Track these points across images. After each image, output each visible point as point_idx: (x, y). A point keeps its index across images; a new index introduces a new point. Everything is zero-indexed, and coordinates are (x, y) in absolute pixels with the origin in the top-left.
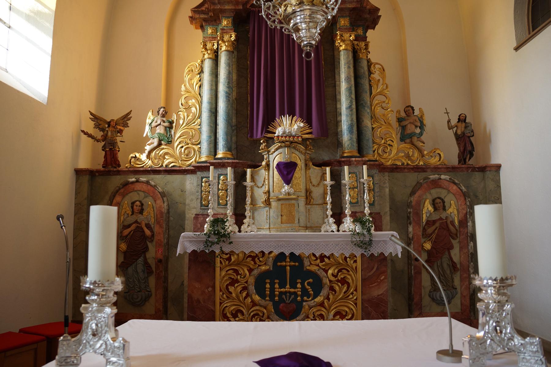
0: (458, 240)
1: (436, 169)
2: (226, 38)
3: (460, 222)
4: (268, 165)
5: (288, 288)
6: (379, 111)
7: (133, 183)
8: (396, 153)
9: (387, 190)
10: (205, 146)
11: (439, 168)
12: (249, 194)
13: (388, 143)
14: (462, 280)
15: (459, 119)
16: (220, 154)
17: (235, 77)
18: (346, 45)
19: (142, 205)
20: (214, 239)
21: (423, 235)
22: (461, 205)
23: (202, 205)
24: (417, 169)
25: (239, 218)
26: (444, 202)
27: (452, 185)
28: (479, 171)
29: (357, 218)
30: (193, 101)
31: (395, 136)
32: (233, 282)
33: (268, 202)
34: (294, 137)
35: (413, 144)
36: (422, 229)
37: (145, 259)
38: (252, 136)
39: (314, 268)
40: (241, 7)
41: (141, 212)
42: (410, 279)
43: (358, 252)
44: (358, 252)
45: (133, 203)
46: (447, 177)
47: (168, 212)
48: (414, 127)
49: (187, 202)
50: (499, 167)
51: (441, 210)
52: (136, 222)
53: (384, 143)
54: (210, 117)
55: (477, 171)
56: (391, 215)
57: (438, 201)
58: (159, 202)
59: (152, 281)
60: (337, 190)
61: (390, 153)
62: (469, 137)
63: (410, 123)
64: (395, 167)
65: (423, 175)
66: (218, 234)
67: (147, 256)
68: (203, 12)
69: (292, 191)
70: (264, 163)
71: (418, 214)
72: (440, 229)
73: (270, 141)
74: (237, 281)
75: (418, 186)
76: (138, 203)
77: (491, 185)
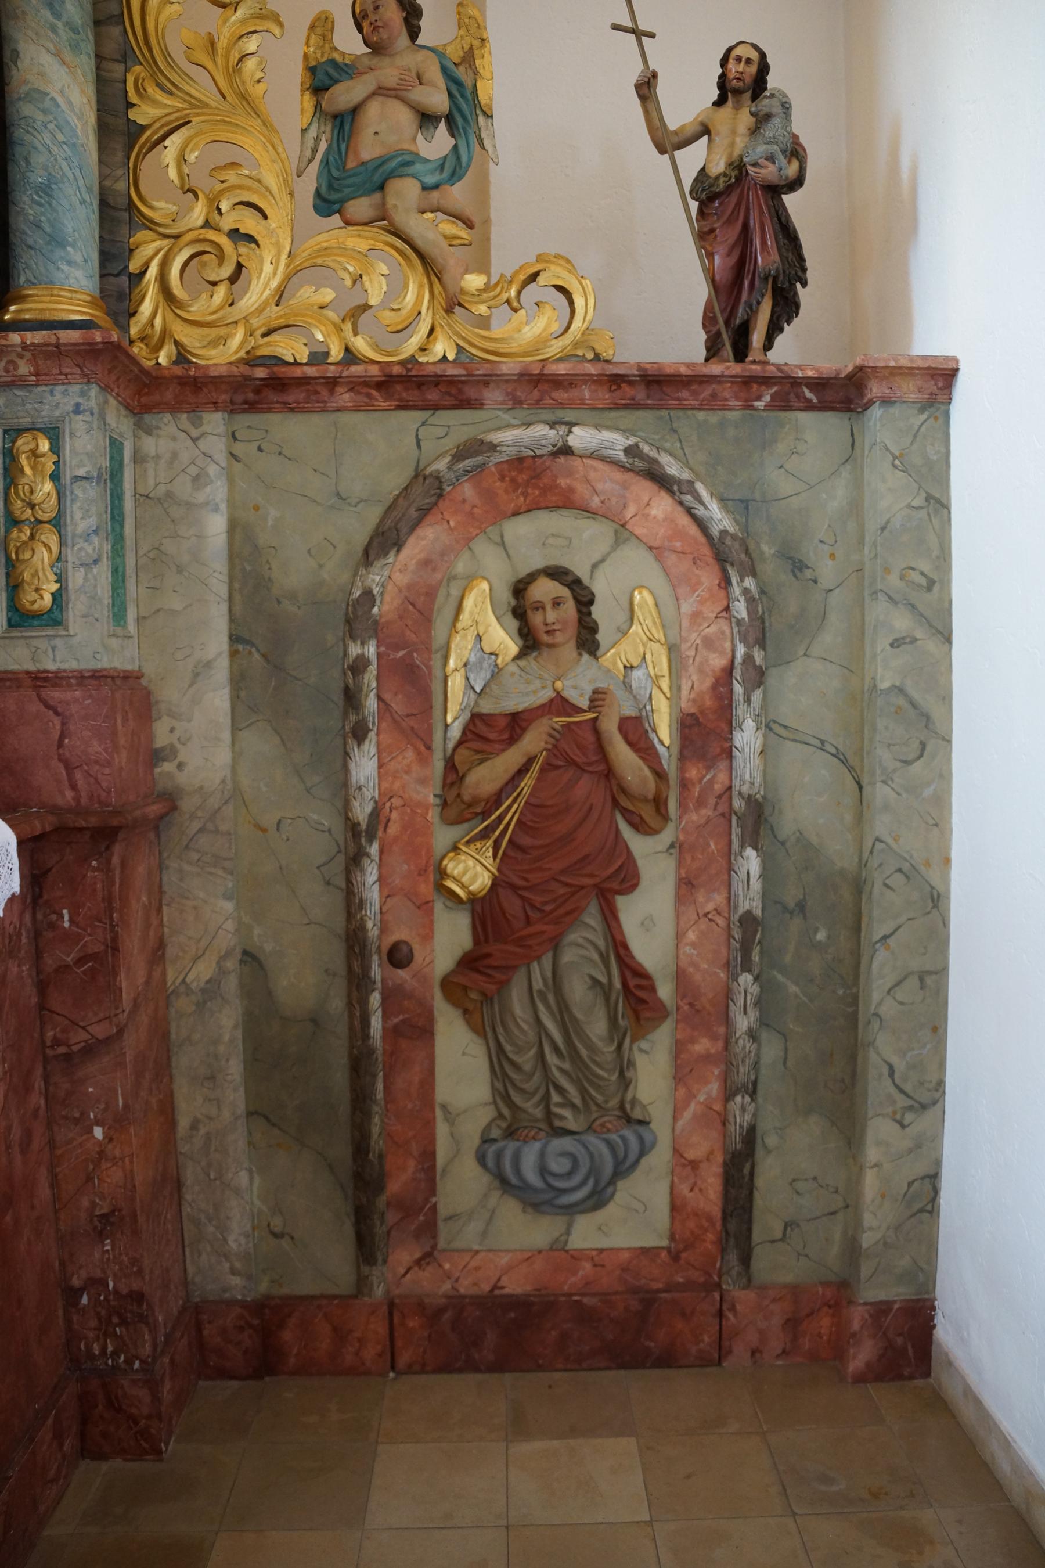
0: (667, 836)
1: (541, 387)
3: (689, 726)
9: (216, 525)
11: (557, 382)
13: (227, 223)
14: (683, 1072)
15: (723, 83)
21: (445, 804)
22: (696, 616)
24: (410, 387)
27: (644, 489)
28: (823, 407)
36: (439, 765)
42: (359, 1064)
46: (615, 442)
48: (405, 117)
50: (942, 377)
51: (569, 650)
53: (207, 225)
55: (809, 407)
56: (238, 681)
57: (544, 589)
62: (775, 191)
63: (381, 91)
64: (260, 373)
65: (456, 426)
71: (413, 675)
72: (548, 767)
75: (423, 497)
77: (888, 494)
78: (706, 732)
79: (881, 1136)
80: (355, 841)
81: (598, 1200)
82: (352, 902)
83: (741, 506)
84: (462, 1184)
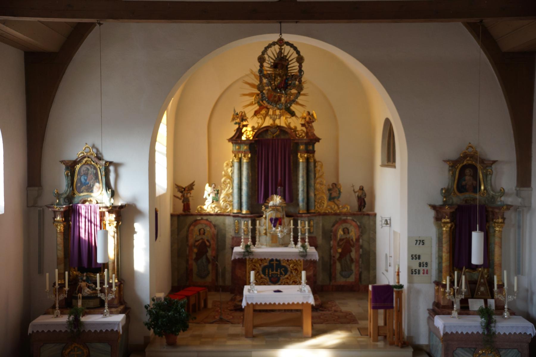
1: (345, 214)
2: (247, 155)
4: (266, 218)
5: (274, 272)
6: (318, 186)
7: (199, 220)
8: (326, 206)
9: (321, 225)
10: (236, 205)
12: (257, 229)
16: (244, 211)
17: (250, 172)
19: (204, 230)
20: (247, 253)
24: (336, 214)
25: (254, 242)
30: (229, 180)
31: (326, 198)
33: (266, 234)
38: (258, 202)
39: (284, 264)
40: (253, 142)
41: (204, 234)
43: (302, 259)
45: (200, 230)
49: (227, 229)
52: (202, 239)
54: (238, 191)
58: (213, 229)
59: (210, 267)
60: (296, 231)
61: (323, 207)
66: (247, 251)
70: (264, 216)
71: (336, 236)
73: (267, 207)
76: (202, 230)
77: (372, 223)
78: (358, 240)
79: (371, 272)
80: (331, 248)
81: (349, 277)
82: (330, 252)
83: (360, 223)
84: (338, 275)
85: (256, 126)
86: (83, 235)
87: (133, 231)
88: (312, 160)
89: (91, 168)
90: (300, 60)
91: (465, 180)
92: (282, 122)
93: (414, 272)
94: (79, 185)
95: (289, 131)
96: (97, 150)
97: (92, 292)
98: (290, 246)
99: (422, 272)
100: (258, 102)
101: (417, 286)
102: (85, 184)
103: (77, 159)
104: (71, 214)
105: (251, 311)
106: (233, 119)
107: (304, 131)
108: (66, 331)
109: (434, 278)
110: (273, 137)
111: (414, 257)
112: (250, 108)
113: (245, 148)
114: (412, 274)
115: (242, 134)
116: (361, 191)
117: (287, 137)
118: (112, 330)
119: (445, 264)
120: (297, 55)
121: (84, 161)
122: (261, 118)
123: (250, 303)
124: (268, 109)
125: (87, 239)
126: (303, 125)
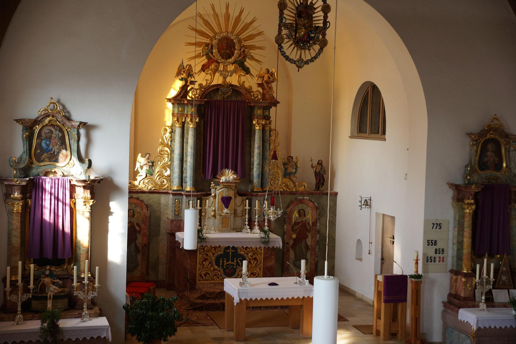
1: (302, 194)
3: (313, 223)
4: (215, 196)
5: (230, 262)
8: (279, 183)
14: (311, 255)
18: (260, 127)
19: (134, 212)
23: (175, 215)
24: (292, 193)
26: (304, 212)
27: (310, 202)
29: (261, 229)
31: (281, 173)
32: (205, 260)
33: (214, 216)
34: (231, 183)
35: (290, 179)
37: (136, 244)
39: (242, 253)
42: (283, 254)
43: (263, 246)
44: (263, 246)
46: (308, 198)
47: (150, 216)
49: (162, 210)
57: (302, 211)
58: (145, 210)
61: (277, 184)
65: (295, 196)
67: (137, 242)
68: (179, 100)
69: (229, 212)
70: (213, 195)
71: (290, 218)
73: (218, 184)
74: (207, 259)
78: (314, 224)
83: (318, 204)
85: (204, 84)
86: (47, 216)
87: (108, 212)
88: (268, 128)
89: (56, 130)
90: (326, 9)
91: (487, 157)
92: (233, 80)
93: (430, 260)
94: (38, 151)
95: (243, 91)
96: (64, 107)
97: (60, 290)
98: (244, 230)
99: (437, 259)
100: (207, 54)
101: (432, 275)
102: (47, 151)
103: (38, 117)
104: (33, 189)
105: (244, 308)
106: (179, 74)
107: (260, 93)
108: (38, 341)
109: (449, 267)
110: (224, 98)
111: (430, 243)
112: (198, 60)
113: (190, 110)
114: (427, 262)
115: (187, 93)
116: (319, 167)
117: (240, 98)
118: (99, 337)
119: (467, 250)
120: (322, 3)
121: (47, 121)
122: (210, 74)
123: (243, 299)
124: (218, 63)
125: (52, 221)
126: (260, 85)
